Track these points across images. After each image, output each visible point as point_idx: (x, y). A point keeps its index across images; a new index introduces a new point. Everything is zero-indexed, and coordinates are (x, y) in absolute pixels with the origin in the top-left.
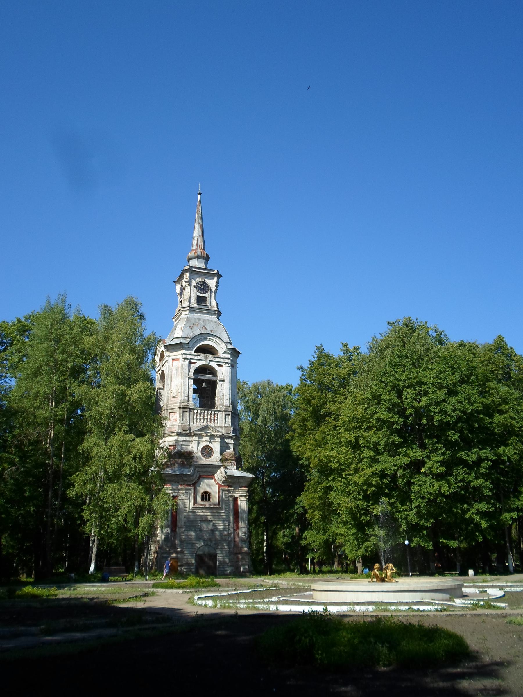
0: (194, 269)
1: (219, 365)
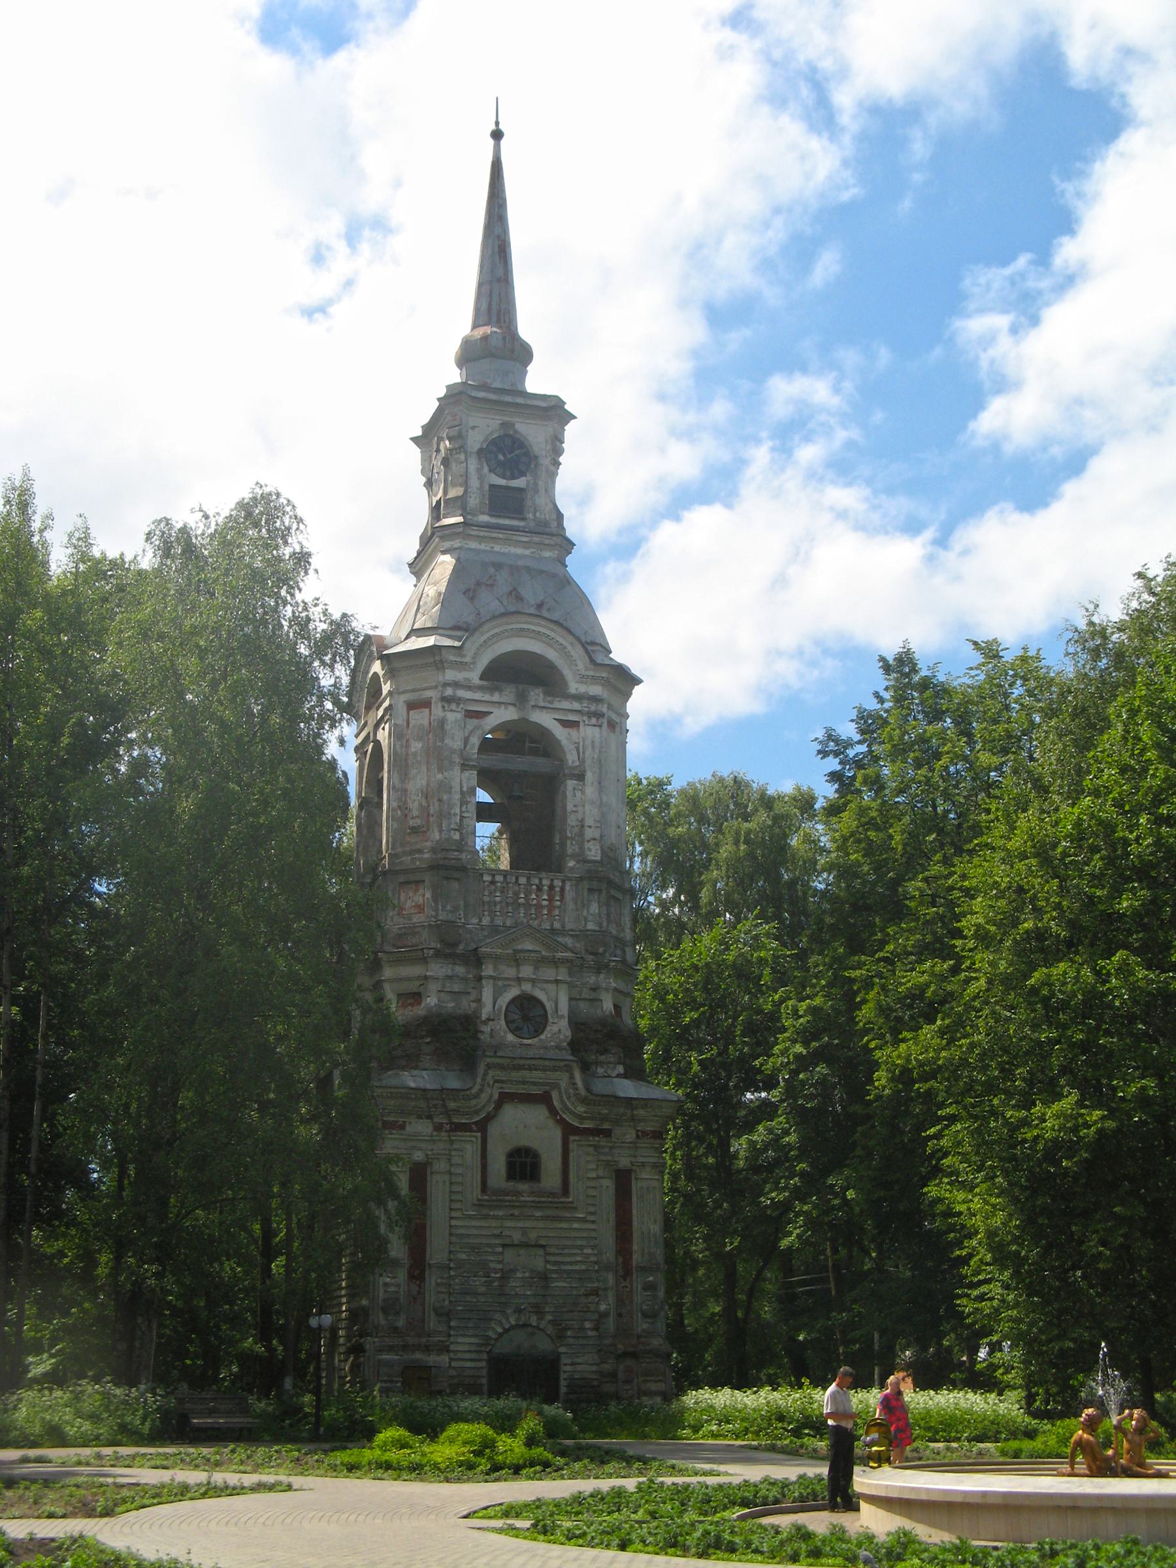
0: (474, 394)
1: (565, 724)
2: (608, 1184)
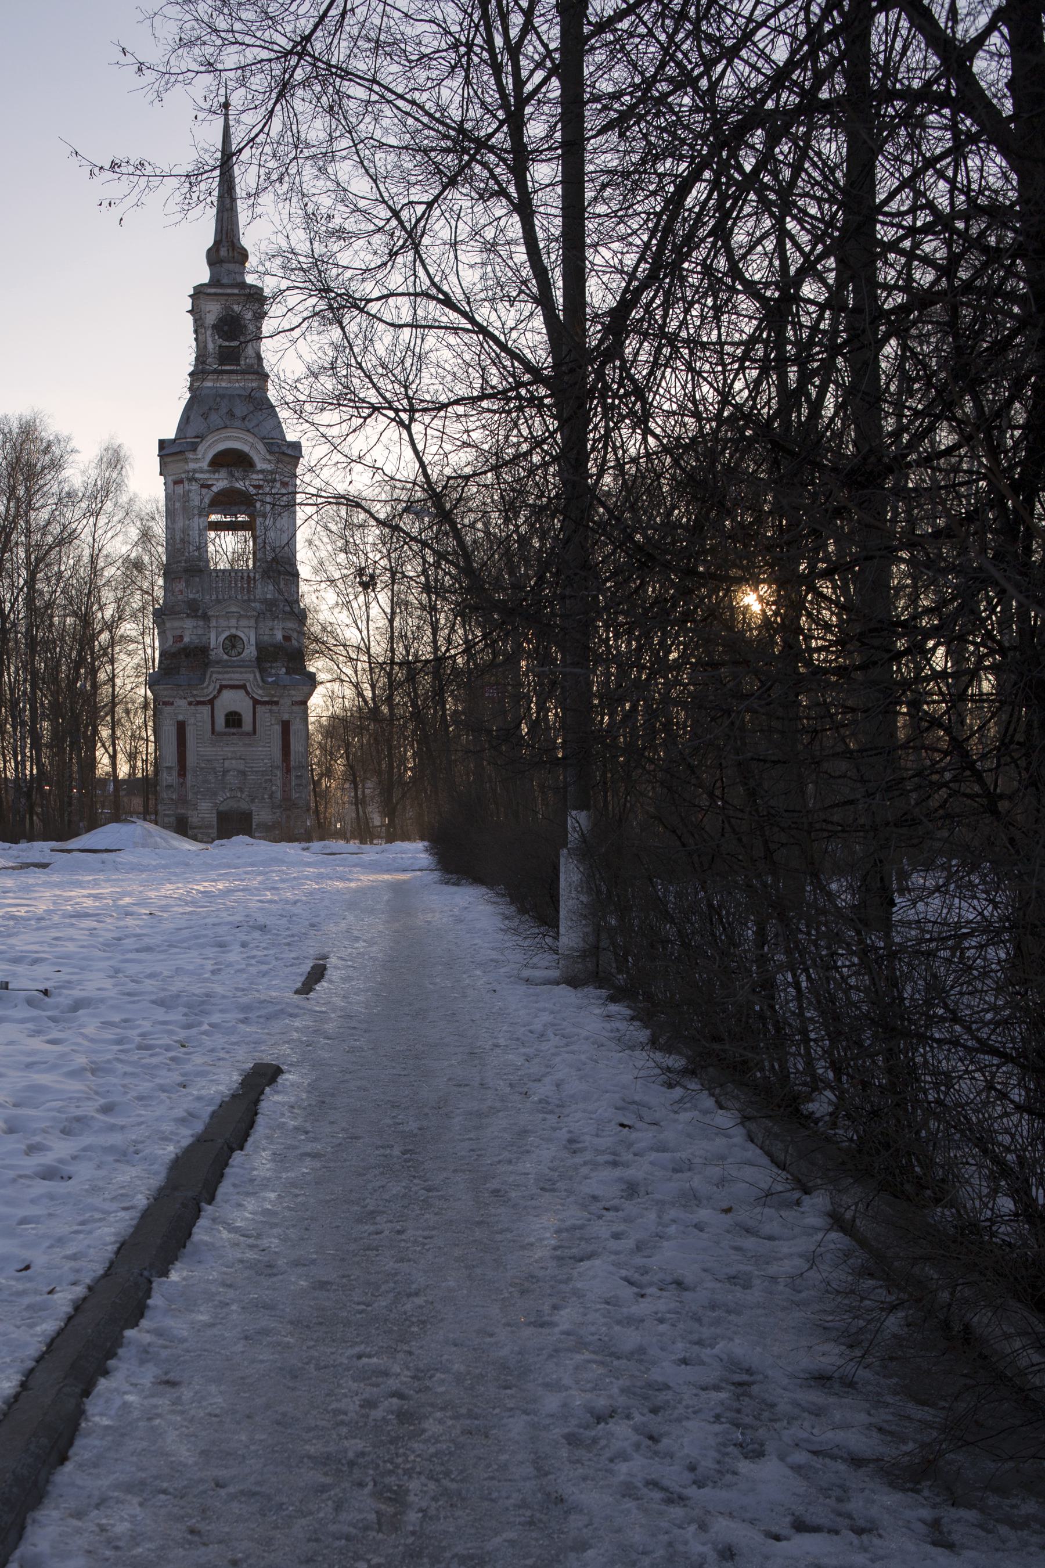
2: (278, 729)
